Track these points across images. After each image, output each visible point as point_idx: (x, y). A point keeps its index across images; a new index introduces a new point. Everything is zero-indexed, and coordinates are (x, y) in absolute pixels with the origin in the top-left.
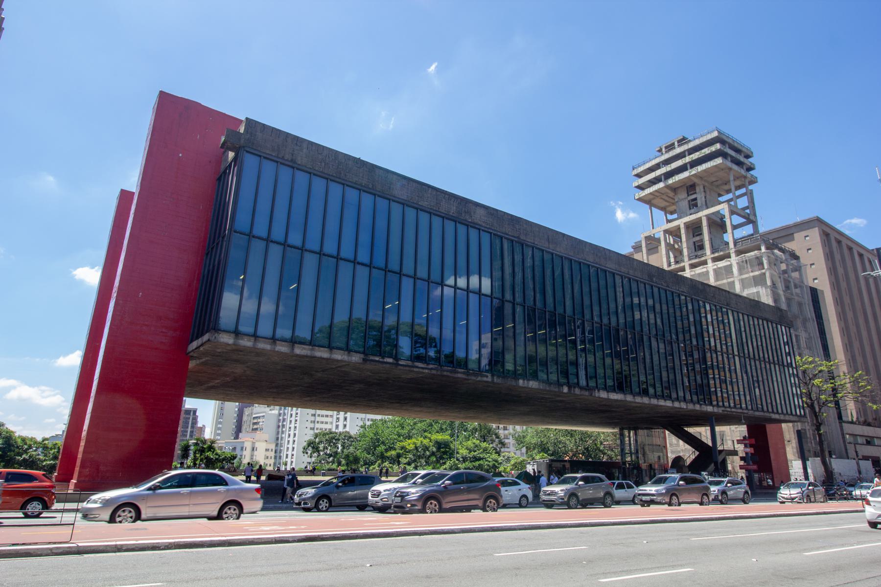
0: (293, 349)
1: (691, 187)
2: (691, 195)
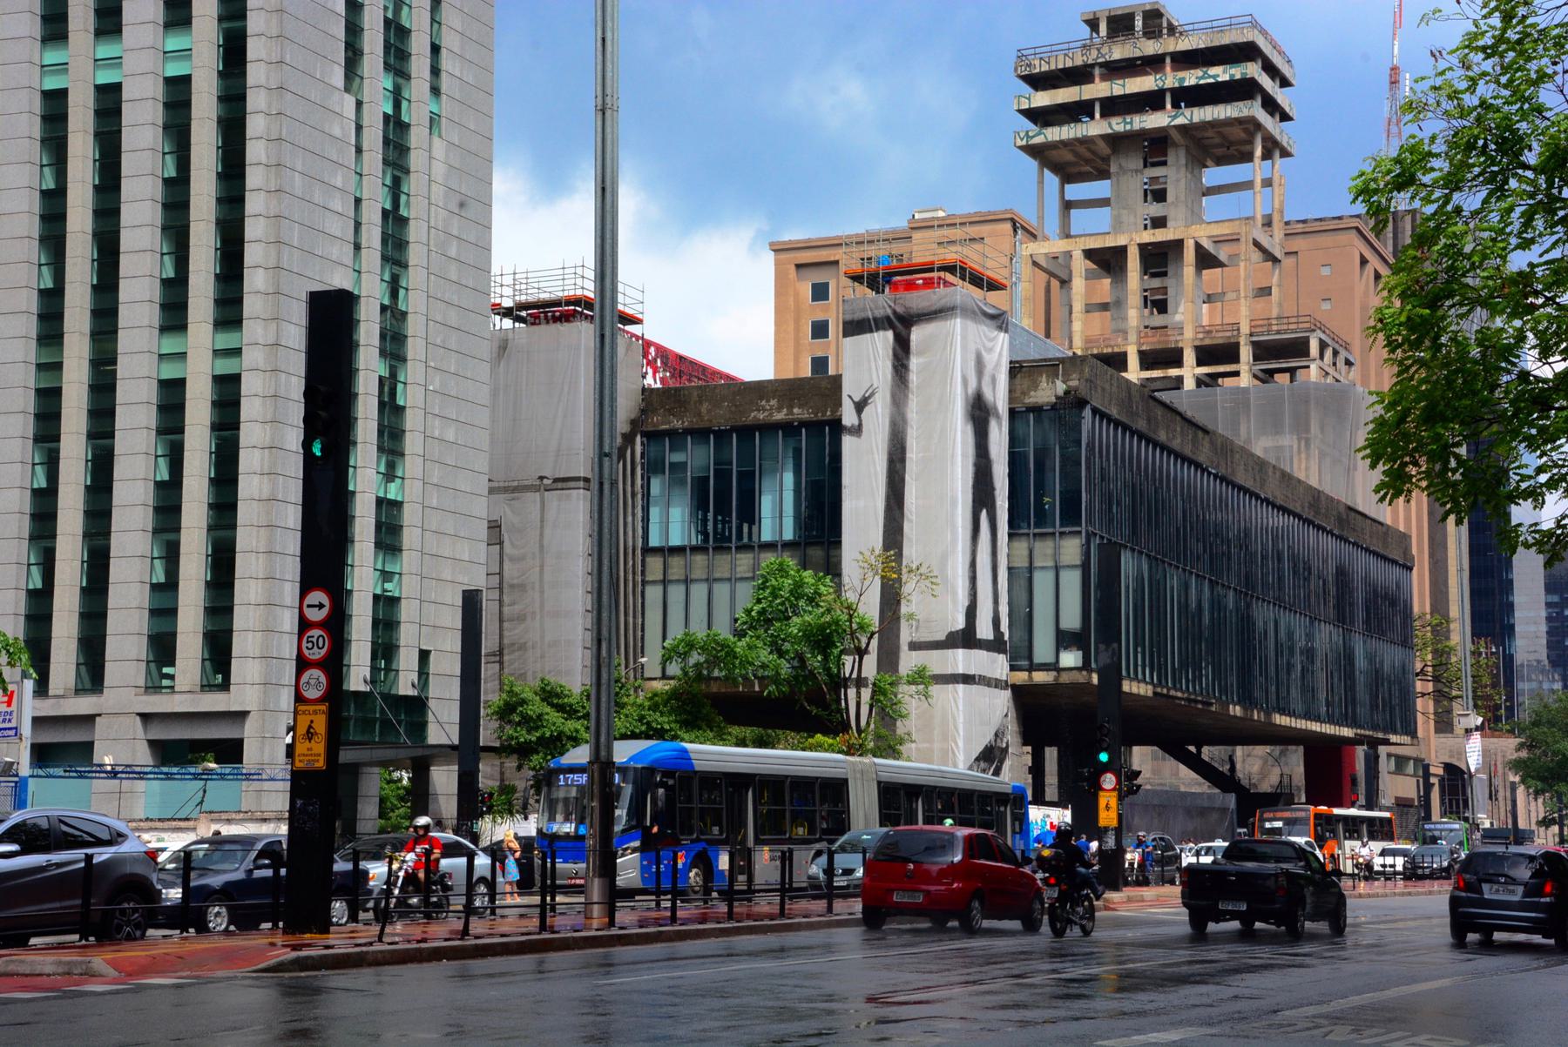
1: (1155, 146)
2: (1154, 165)
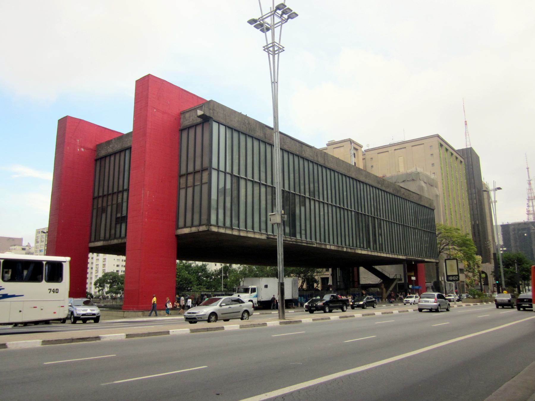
0: (240, 233)
